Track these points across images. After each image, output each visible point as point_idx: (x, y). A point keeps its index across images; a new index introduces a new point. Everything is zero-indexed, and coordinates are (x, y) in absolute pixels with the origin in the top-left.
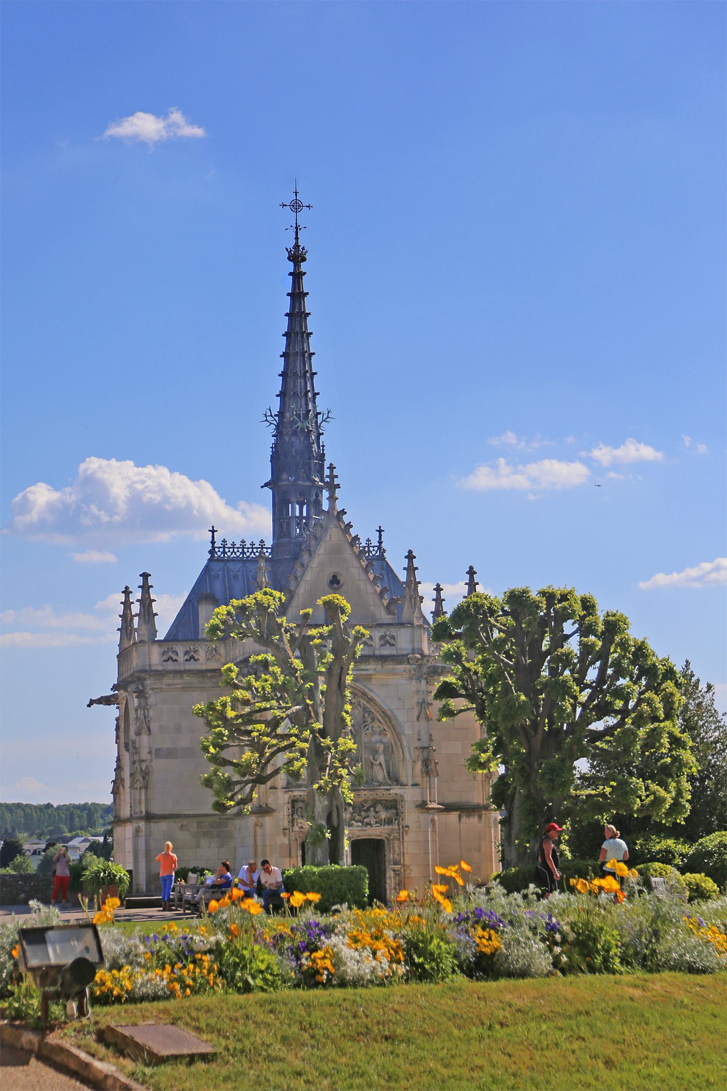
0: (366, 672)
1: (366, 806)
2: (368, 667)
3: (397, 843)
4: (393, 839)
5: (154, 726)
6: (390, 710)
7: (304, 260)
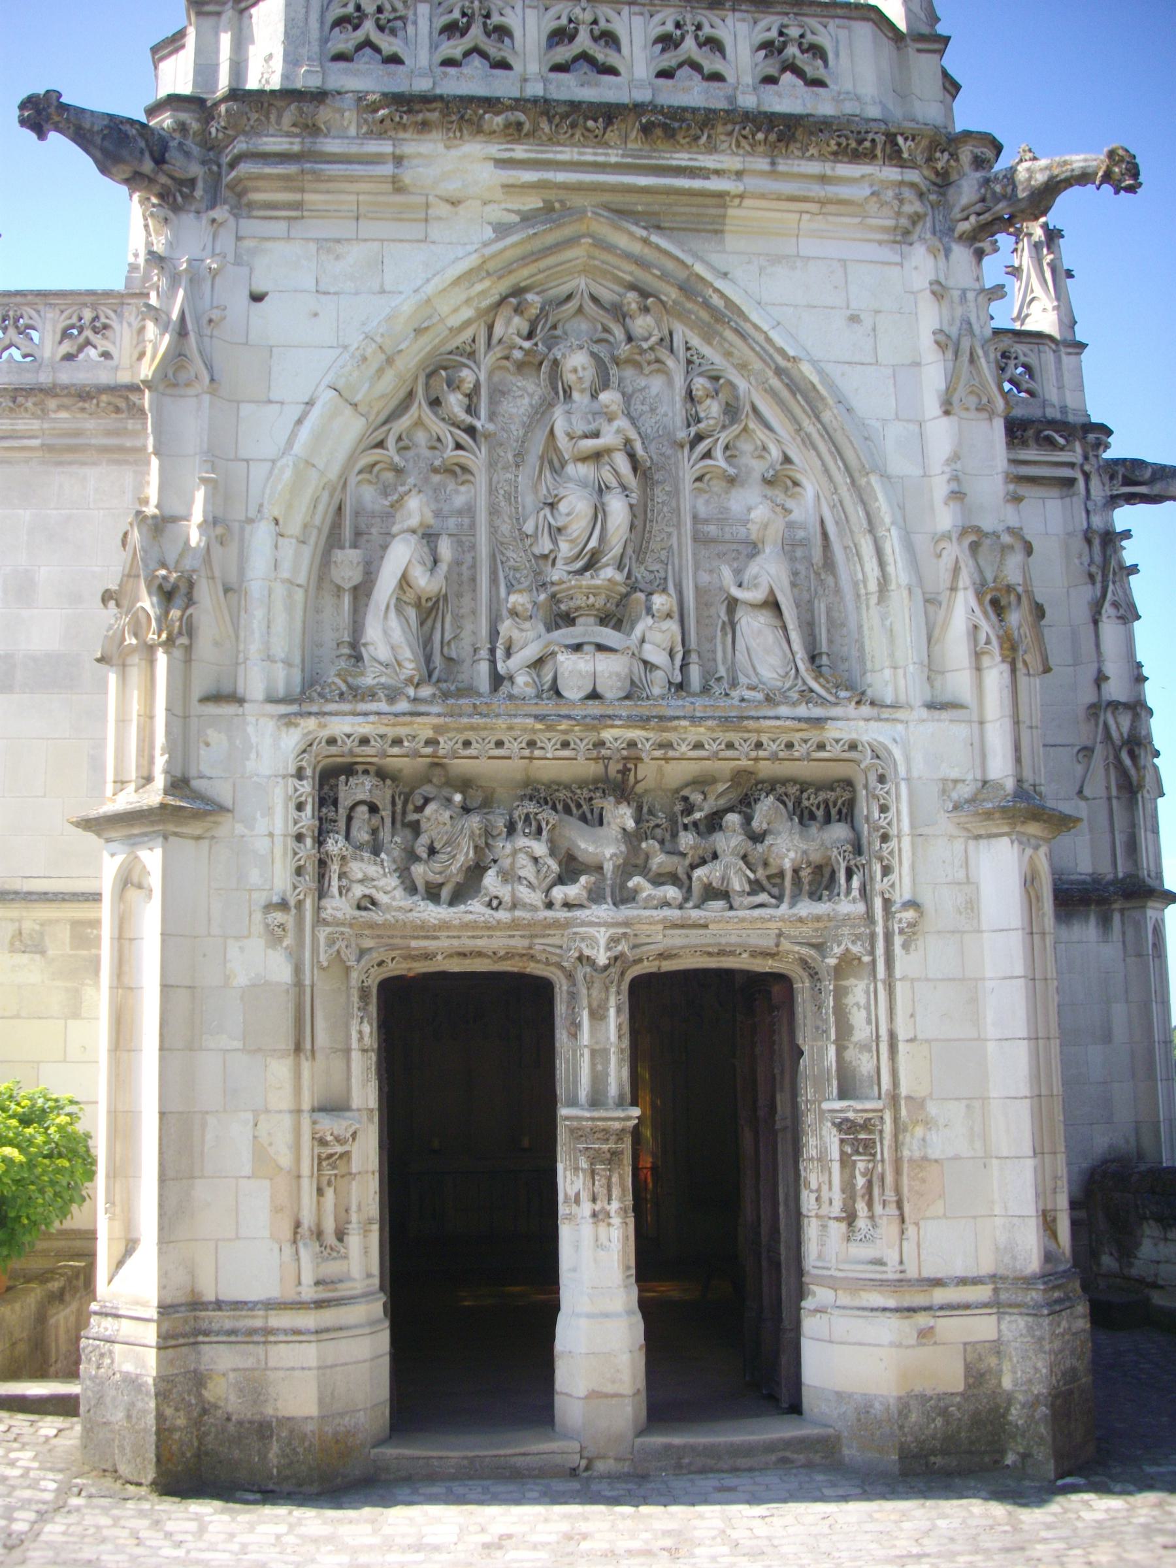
0: (697, 184)
2: (708, 161)
3: (858, 991)
4: (839, 972)
6: (814, 363)
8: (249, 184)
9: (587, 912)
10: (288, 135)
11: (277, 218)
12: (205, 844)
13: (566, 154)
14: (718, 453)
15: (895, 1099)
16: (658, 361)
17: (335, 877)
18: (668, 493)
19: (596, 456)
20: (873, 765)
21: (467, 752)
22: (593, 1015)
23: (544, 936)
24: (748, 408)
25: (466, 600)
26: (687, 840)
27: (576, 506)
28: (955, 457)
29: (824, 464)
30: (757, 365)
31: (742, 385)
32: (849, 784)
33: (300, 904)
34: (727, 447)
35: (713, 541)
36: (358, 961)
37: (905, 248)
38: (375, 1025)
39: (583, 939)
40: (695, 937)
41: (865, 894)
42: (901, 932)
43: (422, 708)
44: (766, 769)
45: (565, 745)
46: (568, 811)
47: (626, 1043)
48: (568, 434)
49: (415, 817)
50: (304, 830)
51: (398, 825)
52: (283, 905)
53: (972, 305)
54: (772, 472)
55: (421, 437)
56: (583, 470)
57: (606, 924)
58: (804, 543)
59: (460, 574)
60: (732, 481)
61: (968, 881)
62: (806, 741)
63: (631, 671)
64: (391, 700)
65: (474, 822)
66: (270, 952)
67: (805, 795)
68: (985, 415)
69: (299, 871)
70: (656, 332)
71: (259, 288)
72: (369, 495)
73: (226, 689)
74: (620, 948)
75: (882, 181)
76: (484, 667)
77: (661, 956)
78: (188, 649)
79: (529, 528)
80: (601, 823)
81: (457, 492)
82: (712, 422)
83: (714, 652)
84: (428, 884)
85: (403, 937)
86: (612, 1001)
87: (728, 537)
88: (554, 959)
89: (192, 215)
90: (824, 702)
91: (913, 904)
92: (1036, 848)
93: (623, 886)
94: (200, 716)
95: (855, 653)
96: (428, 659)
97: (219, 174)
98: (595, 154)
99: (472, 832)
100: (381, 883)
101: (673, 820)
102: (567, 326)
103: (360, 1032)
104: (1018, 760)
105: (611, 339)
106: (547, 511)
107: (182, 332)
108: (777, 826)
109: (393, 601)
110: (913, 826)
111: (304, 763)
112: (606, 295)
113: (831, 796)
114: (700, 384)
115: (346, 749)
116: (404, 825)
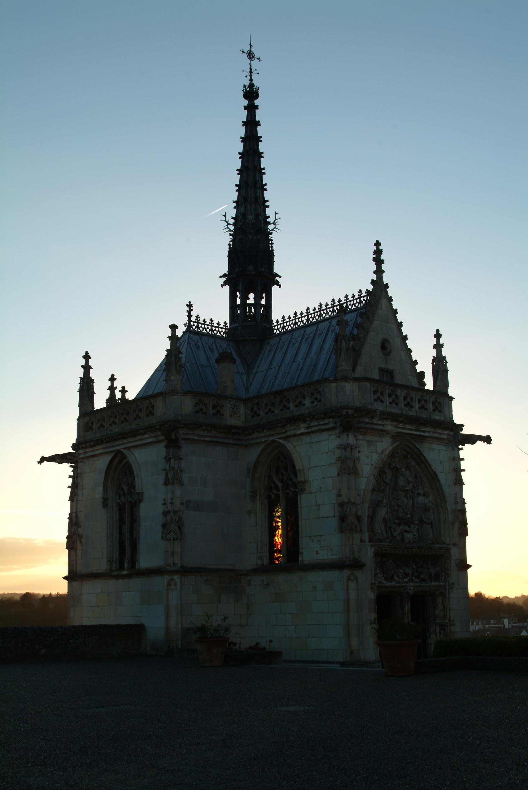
5: (185, 477)
7: (257, 96)
15: (450, 620)
19: (406, 491)
79: (392, 504)
91: (453, 584)
107: (354, 462)
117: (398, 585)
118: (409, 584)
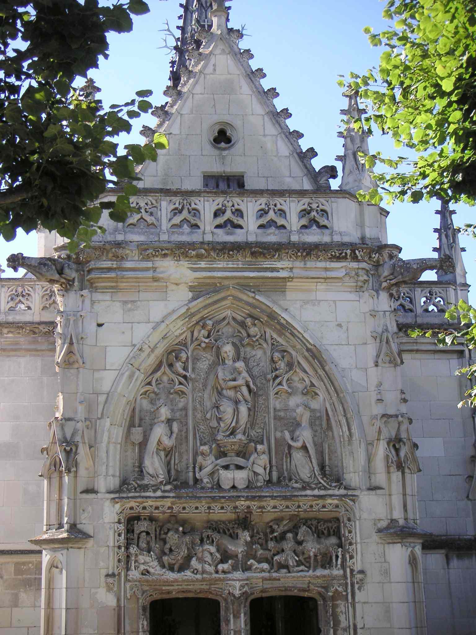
0: (275, 274)
1: (279, 530)
2: (279, 265)
3: (342, 606)
4: (333, 598)
8: (96, 280)
9: (232, 575)
10: (111, 260)
11: (107, 292)
12: (83, 550)
13: (221, 265)
14: (284, 383)
16: (260, 344)
17: (133, 562)
18: (264, 400)
19: (236, 388)
20: (346, 514)
21: (184, 512)
22: (234, 616)
23: (214, 584)
24: (296, 363)
25: (184, 446)
26: (271, 544)
27: (227, 409)
28: (380, 384)
29: (326, 388)
30: (299, 347)
31: (294, 353)
32: (338, 519)
33: (119, 574)
34: (288, 380)
35: (283, 418)
36: (142, 595)
37: (361, 293)
38: (149, 620)
39: (230, 586)
40: (276, 584)
41: (343, 567)
42: (357, 583)
43: (166, 494)
44: (302, 515)
45: (222, 508)
46: (225, 533)
47: (248, 627)
48: (223, 380)
49: (164, 536)
50: (121, 544)
51: (158, 539)
52: (113, 575)
53: (388, 318)
54: (306, 390)
55: (165, 379)
56: (231, 393)
57: (239, 580)
58: (320, 418)
59: (181, 435)
60: (290, 394)
61: (385, 562)
62: (318, 505)
63: (248, 476)
64: (155, 491)
65: (187, 539)
66: (108, 593)
67: (319, 524)
68: (392, 365)
69: (119, 561)
70: (259, 334)
71: (100, 322)
72: (145, 404)
73: (90, 487)
74: (245, 589)
75: (350, 268)
76: (191, 474)
77: (262, 591)
78: (76, 472)
80: (237, 538)
81: (180, 401)
82: (281, 371)
83: (283, 465)
84: (169, 564)
85: (159, 585)
86: (242, 611)
87: (288, 416)
88: (220, 593)
89: (73, 292)
90: (325, 489)
91: (362, 572)
92: (414, 547)
93: (246, 563)
94: (80, 499)
95: (340, 464)
96: (169, 472)
97: (84, 275)
98: (233, 264)
99: (187, 543)
100: (151, 564)
101: (266, 535)
102: (224, 330)
103: (143, 624)
104: (406, 510)
105: (241, 335)
106: (215, 409)
107: (71, 343)
108: (307, 538)
109: (155, 450)
110: (361, 539)
111: (121, 518)
112: (239, 318)
113: (330, 525)
114: (277, 355)
115: (137, 511)
116: (160, 539)
117: (199, 576)
118: (229, 576)
